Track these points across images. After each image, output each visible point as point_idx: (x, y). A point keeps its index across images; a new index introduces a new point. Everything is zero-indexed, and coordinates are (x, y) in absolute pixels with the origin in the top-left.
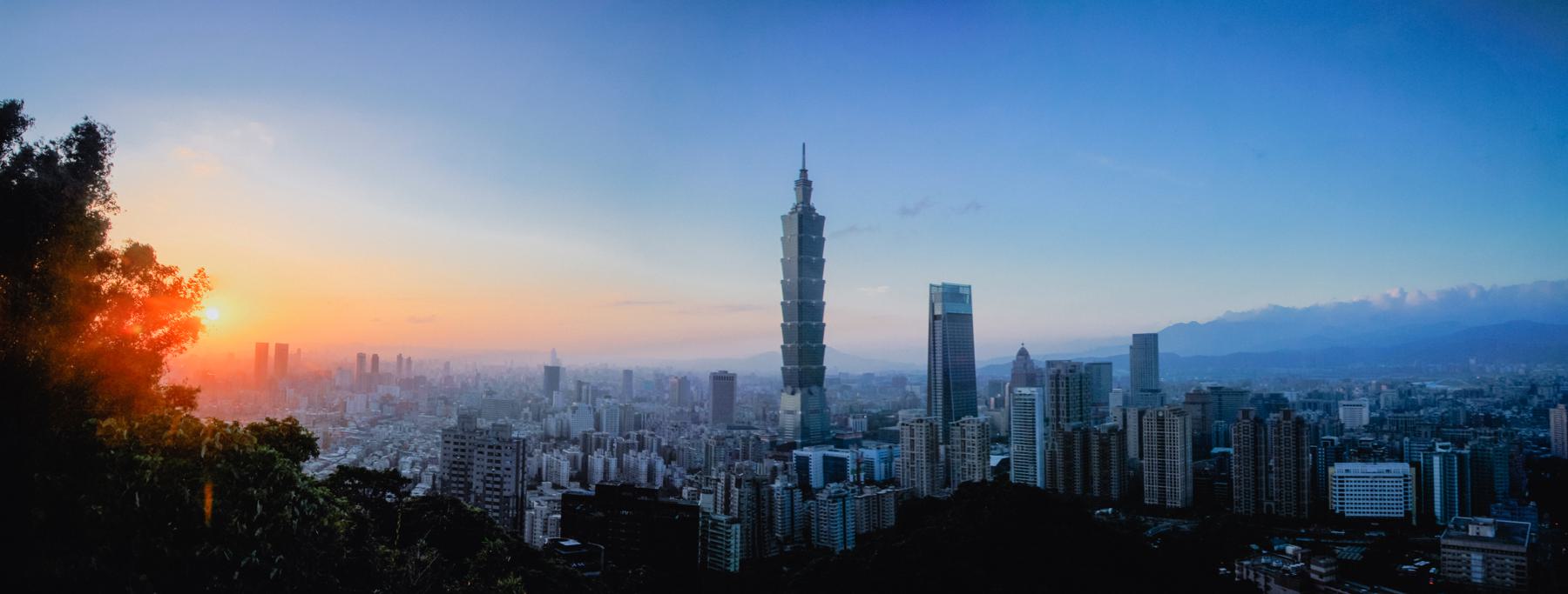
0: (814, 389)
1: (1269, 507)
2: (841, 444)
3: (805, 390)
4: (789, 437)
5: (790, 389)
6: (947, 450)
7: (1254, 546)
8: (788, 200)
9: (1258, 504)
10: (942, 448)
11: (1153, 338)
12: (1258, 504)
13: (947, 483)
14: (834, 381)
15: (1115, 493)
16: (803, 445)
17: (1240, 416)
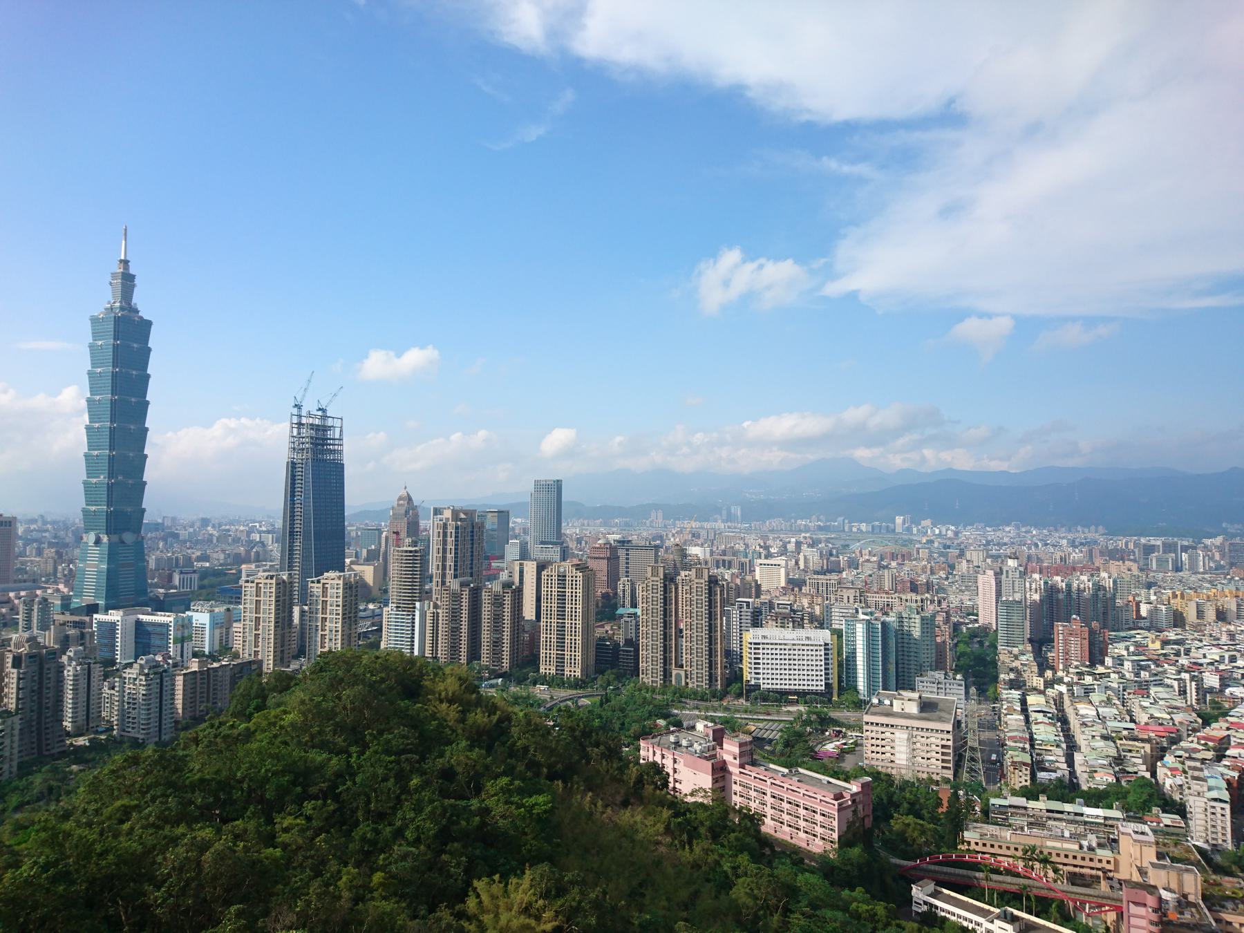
0: (128, 537)
1: (678, 675)
2: (160, 606)
3: (115, 538)
4: (88, 599)
5: (90, 538)
6: (302, 612)
7: (661, 722)
8: (103, 299)
9: (667, 674)
10: (296, 610)
11: (557, 487)
12: (667, 674)
13: (301, 652)
14: (157, 527)
15: (506, 664)
16: (107, 609)
17: (649, 575)
